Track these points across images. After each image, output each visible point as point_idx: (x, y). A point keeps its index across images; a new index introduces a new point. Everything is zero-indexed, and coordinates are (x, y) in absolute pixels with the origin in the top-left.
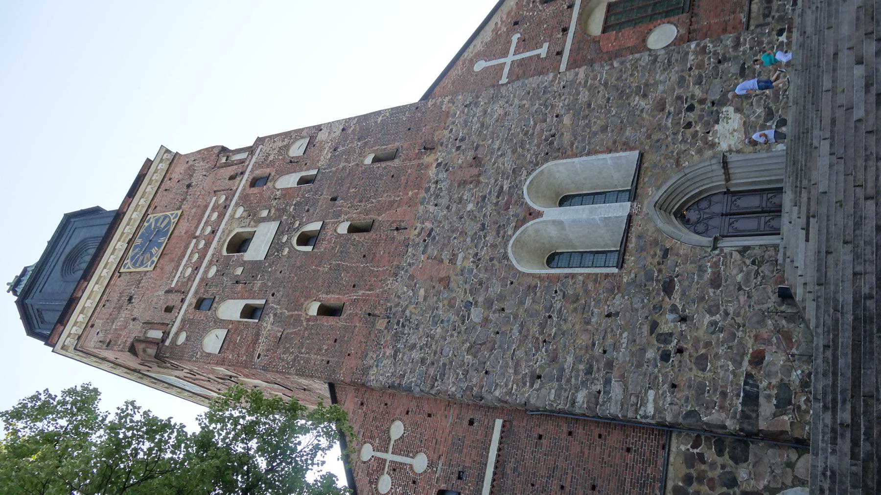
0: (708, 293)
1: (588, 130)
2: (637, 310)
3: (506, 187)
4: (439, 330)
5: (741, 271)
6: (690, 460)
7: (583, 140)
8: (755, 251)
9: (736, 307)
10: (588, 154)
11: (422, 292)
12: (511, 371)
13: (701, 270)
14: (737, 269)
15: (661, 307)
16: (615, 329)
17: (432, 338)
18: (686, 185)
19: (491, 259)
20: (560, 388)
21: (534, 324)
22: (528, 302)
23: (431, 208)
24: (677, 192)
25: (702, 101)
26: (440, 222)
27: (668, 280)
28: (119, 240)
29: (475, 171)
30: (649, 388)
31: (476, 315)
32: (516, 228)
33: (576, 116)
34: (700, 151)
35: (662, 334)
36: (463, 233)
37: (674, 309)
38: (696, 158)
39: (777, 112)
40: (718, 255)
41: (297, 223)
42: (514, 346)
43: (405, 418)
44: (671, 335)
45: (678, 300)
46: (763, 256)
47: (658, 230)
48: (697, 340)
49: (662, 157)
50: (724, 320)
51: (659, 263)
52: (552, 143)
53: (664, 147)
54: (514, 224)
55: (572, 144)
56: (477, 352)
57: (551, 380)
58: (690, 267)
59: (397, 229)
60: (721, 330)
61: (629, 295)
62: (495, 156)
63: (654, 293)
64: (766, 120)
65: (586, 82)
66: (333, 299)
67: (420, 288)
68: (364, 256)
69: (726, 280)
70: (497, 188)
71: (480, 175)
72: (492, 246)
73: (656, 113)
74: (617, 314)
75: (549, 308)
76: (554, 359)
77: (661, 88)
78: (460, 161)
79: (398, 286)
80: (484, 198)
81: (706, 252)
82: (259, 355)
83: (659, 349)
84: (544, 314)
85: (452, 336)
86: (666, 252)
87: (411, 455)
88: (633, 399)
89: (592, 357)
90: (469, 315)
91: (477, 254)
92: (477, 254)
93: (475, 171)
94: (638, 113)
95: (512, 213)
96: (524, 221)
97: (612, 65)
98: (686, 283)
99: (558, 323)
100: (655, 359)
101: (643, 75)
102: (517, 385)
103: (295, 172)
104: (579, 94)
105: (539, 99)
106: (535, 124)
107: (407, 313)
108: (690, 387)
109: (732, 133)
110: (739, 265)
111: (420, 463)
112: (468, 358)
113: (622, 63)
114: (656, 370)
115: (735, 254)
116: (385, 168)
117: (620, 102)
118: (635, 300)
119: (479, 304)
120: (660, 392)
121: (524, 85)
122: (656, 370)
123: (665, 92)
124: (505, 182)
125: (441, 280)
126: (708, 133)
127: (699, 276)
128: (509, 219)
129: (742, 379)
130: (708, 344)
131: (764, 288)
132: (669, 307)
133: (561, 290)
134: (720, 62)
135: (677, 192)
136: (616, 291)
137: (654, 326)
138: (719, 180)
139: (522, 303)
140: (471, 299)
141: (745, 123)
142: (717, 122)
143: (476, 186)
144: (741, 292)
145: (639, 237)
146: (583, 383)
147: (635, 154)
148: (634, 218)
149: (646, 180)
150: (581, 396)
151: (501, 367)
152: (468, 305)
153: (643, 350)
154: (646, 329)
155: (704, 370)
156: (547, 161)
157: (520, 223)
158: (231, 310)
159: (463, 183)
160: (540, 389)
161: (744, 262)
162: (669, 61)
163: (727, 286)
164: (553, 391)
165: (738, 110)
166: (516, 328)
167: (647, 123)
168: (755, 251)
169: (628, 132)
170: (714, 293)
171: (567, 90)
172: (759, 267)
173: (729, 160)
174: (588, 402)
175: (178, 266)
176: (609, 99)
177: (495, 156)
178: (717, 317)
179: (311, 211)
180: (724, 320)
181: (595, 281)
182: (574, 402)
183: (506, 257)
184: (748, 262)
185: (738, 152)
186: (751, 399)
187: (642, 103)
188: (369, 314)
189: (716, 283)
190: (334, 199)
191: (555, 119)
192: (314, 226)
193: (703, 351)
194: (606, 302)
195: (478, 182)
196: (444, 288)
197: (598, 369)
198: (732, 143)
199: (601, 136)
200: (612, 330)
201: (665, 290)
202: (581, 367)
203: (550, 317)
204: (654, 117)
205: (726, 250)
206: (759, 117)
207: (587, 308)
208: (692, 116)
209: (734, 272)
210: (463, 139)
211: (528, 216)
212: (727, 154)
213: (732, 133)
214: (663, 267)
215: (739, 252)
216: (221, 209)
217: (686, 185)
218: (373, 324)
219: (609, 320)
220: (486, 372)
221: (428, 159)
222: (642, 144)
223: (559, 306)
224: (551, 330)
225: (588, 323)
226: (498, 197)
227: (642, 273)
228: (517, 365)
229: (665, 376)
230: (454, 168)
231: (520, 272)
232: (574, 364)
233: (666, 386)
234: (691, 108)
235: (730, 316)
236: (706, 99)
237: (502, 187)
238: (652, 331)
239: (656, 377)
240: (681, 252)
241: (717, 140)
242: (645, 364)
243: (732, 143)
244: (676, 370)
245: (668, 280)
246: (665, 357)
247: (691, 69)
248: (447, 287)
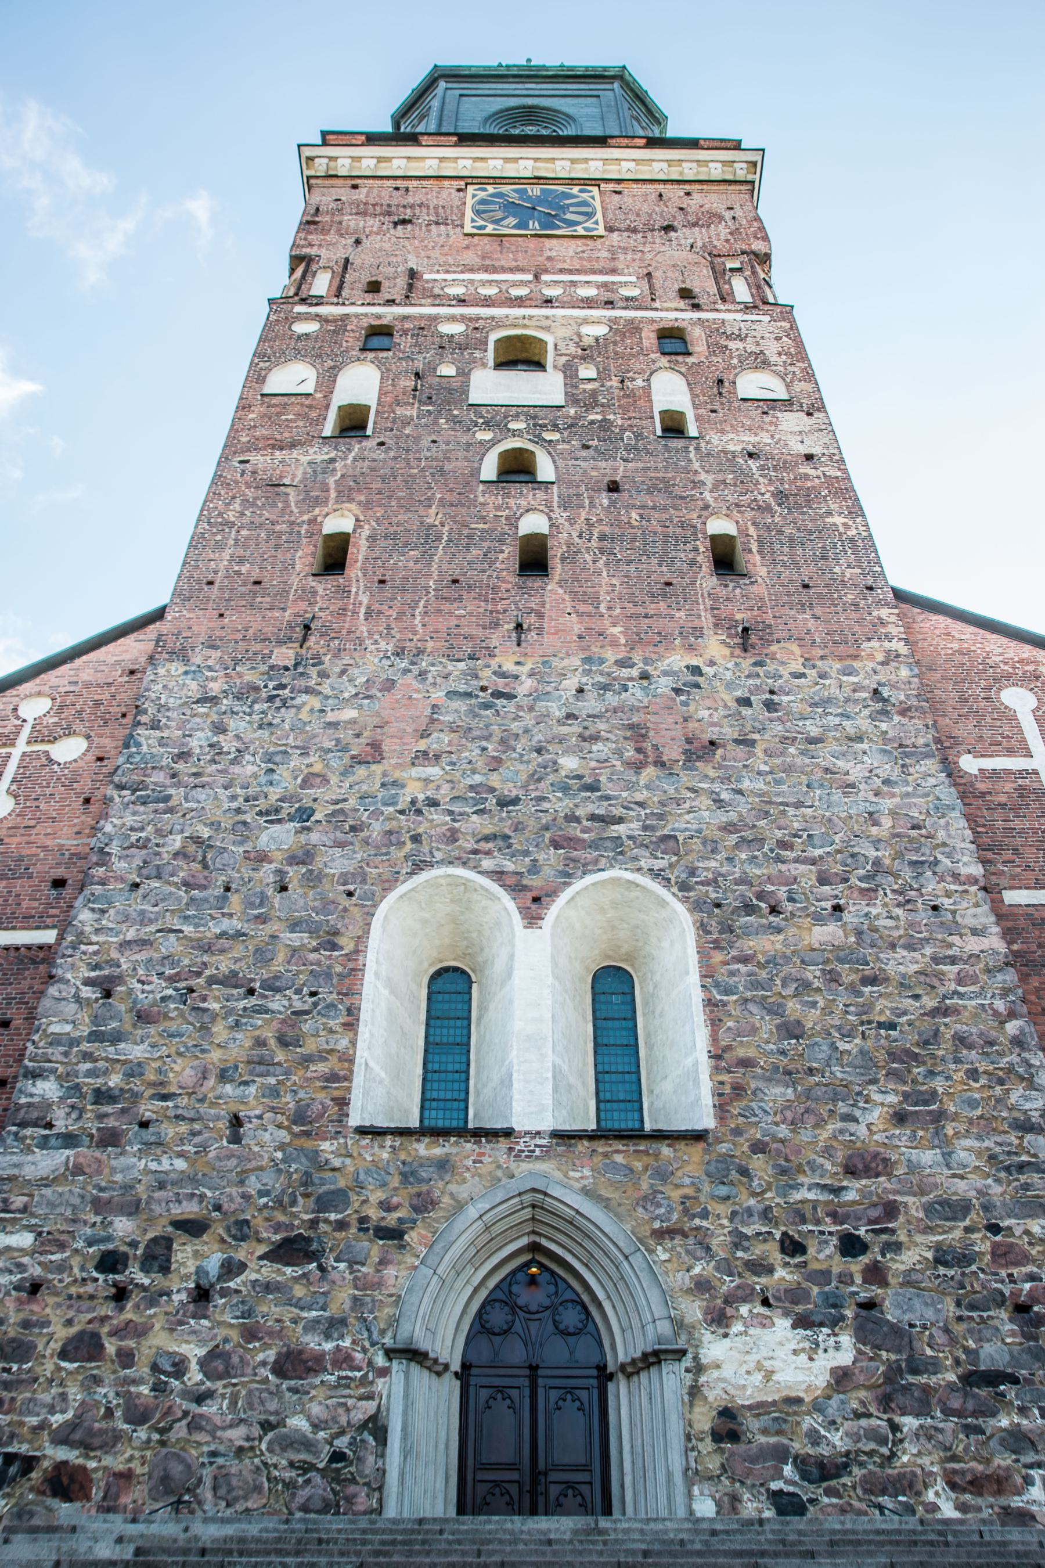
0: (266, 1347)
1: (790, 991)
2: (242, 1182)
3: (620, 829)
4: (250, 769)
5: (316, 1427)
7: (756, 985)
8: (371, 1459)
9: (218, 1420)
10: (709, 1003)
11: (349, 714)
12: (131, 935)
13: (333, 1326)
14: (324, 1415)
15: (243, 1238)
16: (198, 1139)
17: (233, 762)
18: (605, 1261)
19: (416, 839)
20: (74, 1042)
21: (237, 960)
22: (296, 939)
23: (571, 683)
24: (587, 1244)
25: (876, 1274)
26: (531, 709)
27: (314, 1246)
28: (536, 160)
29: (673, 752)
30: (40, 1234)
31: (279, 838)
32: (498, 875)
33: (842, 954)
34: (702, 1286)
35: (169, 1248)
36: (496, 764)
37: (231, 1268)
38: (682, 1279)
39: (829, 1492)
40: (370, 1363)
42: (188, 929)
43: (90, 757)
44: (165, 1269)
45: (254, 1276)
46: (353, 1481)
47: (460, 1206)
48: (141, 1331)
49: (689, 1191)
50: (185, 1394)
51: (363, 1220)
52: (749, 909)
53: (723, 1190)
54: (509, 866)
55: (745, 960)
56: (186, 856)
57: (96, 1020)
58: (342, 1298)
59: (519, 626)
60: (159, 1388)
61: (284, 1160)
62: (716, 787)
63: (281, 1218)
64: (801, 1463)
65: (953, 960)
66: (358, 553)
67: (360, 707)
68: (455, 581)
69: (294, 1391)
70: (618, 811)
71: (660, 764)
72: (454, 831)
73: (840, 1156)
74: (236, 1139)
75: (272, 986)
76: (143, 1017)
77: (928, 1157)
78: (704, 713)
79: (371, 662)
80: (593, 788)
81: (383, 1332)
82: (247, 462)
83: (134, 1244)
84: (258, 976)
85: (234, 798)
86: (394, 1234)
87: (14, 787)
88: (19, 1201)
89: (136, 1096)
90: (280, 821)
91: (433, 803)
92: (433, 803)
93: (673, 752)
94: (842, 1108)
95: (541, 857)
96: (516, 889)
97: (1012, 1015)
98: (299, 1291)
99: (230, 1012)
100: (109, 1239)
101: (973, 1104)
102: (95, 953)
103: (694, 396)
104: (910, 947)
105: (898, 855)
106: (813, 862)
107: (304, 697)
108: (26, 1324)
109: (759, 1367)
110: (335, 1420)
112: (176, 842)
113: (1018, 1042)
114: (80, 1244)
115: (370, 1407)
116: (693, 563)
117: (881, 1056)
118: (269, 1178)
119: (303, 838)
120: (25, 1260)
121: (941, 810)
122: (80, 1244)
123: (913, 1168)
124: (636, 825)
125: (375, 746)
126: (766, 1303)
127: (317, 1321)
128: (526, 853)
129: (24, 1449)
130: (126, 1358)
131: (258, 1489)
132: (241, 1255)
133: (315, 1005)
134: (1021, 1309)
135: (587, 1244)
136: (296, 1129)
137: (194, 1228)
138: (624, 1349)
139: (294, 926)
140: (318, 816)
141: (799, 1401)
142: (802, 1322)
143: (628, 764)
144: (256, 1431)
145: (443, 1165)
146: (77, 1087)
147: (706, 1120)
148: (503, 1144)
149: (619, 1158)
150: (47, 1089)
151: (142, 913)
152: (304, 814)
153: (133, 1208)
154: (190, 1209)
155: (63, 1355)
156: (696, 906)
157: (511, 881)
158: (361, 383)
159: (638, 733)
160: (77, 999)
161: (342, 1433)
162: (1021, 1167)
163: (277, 1393)
164: (68, 1028)
165: (841, 1378)
166: (236, 924)
167: (805, 1136)
168: (371, 1459)
169: (779, 1093)
170: (264, 1363)
171: (923, 916)
172: (323, 1472)
173: (665, 1367)
174: (30, 1105)
176: (892, 1026)
177: (716, 787)
178: (194, 1375)
179: (584, 453)
180: (185, 1394)
181: (333, 1077)
182: (35, 1075)
183: (419, 867)
184: (342, 1443)
185: (695, 1391)
187: (875, 1115)
188: (307, 628)
189: (294, 1365)
190: (613, 487)
191: (828, 905)
192: (545, 469)
193: (111, 1347)
194: (273, 1109)
196: (353, 757)
197: (106, 1115)
198: (727, 1372)
199: (767, 1026)
200: (194, 1134)
201: (286, 1241)
202: (115, 1080)
203: (251, 992)
204: (828, 1152)
205: (380, 1385)
206: (815, 1438)
207: (260, 1069)
208: (824, 1254)
209: (316, 1409)
210: (770, 706)
211: (529, 895)
212: (687, 1362)
213: (759, 1367)
214: (353, 1230)
215: (374, 1418)
216: (608, 296)
217: (605, 1261)
218: (280, 642)
219: (223, 1125)
220: (136, 886)
222: (737, 1132)
223: (274, 1006)
224: (217, 999)
225: (223, 1076)
226: (593, 817)
227: (342, 1184)
228: (144, 943)
229: (62, 1267)
230: (685, 704)
231: (375, 906)
232: (125, 1062)
233: (37, 1271)
234: (851, 1246)
235: (193, 1407)
236: (884, 1283)
237: (620, 820)
238: (181, 1225)
239: (62, 1246)
240: (390, 1271)
241: (737, 1327)
242: (99, 1219)
243: (727, 1372)
244: (73, 1290)
245: (314, 1246)
246: (110, 1262)
247: (994, 1229)
248: (358, 761)
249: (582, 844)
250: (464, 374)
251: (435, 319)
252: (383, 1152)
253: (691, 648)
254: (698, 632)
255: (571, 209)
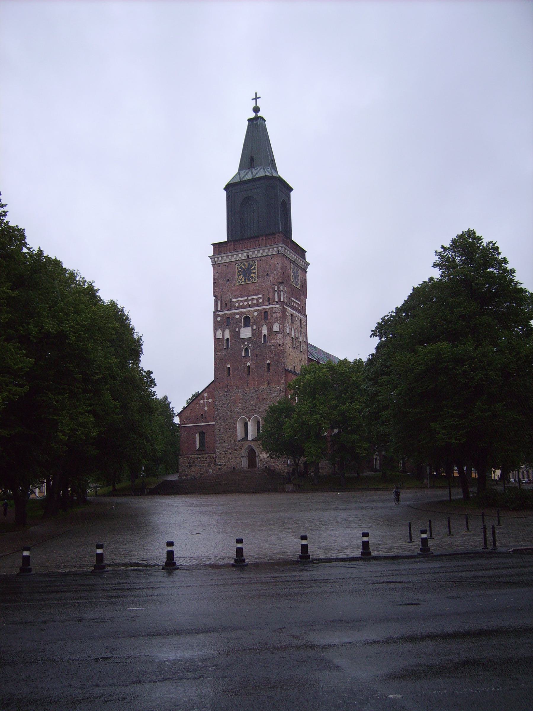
6: (213, 457)
31: (229, 413)
41: (250, 345)
111: (206, 408)
137: (229, 449)
159: (258, 398)
175: (239, 297)
186: (220, 465)
189: (236, 458)
195: (258, 402)
221: (266, 385)
246: (224, 452)
249: (253, 413)
250: (239, 330)
251: (235, 314)
252: (240, 442)
253: (263, 385)
254: (264, 382)
255: (253, 271)
